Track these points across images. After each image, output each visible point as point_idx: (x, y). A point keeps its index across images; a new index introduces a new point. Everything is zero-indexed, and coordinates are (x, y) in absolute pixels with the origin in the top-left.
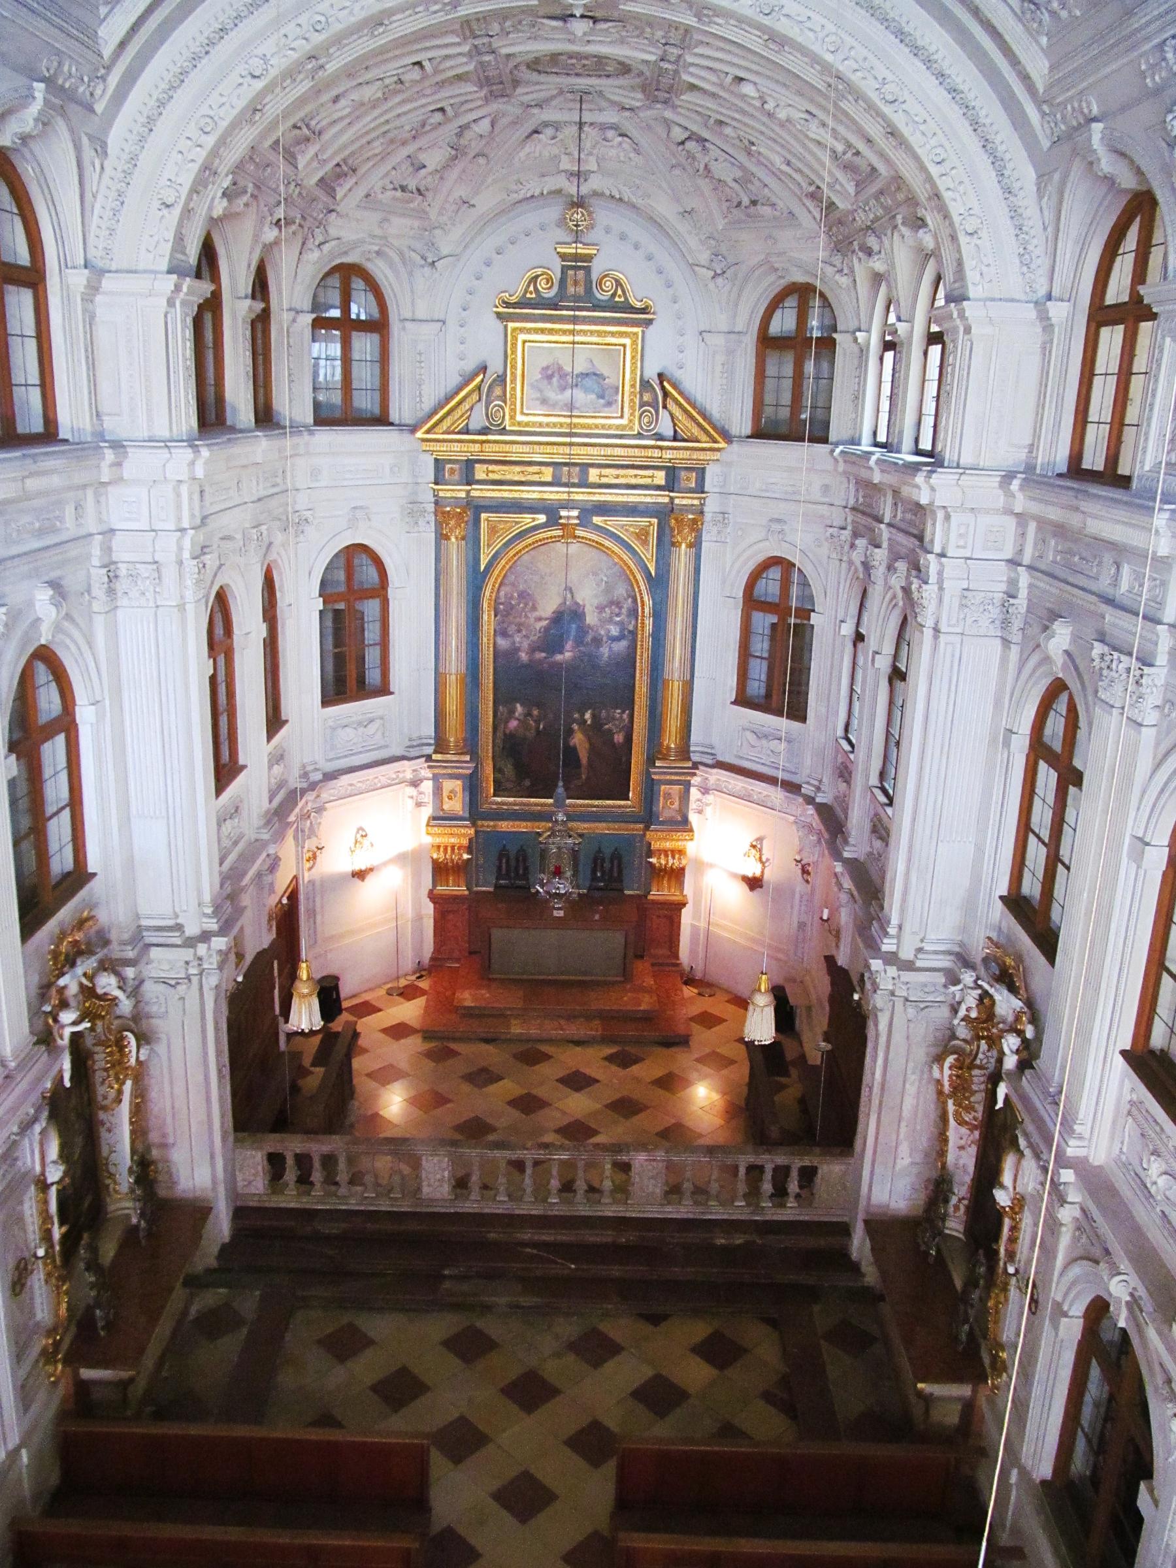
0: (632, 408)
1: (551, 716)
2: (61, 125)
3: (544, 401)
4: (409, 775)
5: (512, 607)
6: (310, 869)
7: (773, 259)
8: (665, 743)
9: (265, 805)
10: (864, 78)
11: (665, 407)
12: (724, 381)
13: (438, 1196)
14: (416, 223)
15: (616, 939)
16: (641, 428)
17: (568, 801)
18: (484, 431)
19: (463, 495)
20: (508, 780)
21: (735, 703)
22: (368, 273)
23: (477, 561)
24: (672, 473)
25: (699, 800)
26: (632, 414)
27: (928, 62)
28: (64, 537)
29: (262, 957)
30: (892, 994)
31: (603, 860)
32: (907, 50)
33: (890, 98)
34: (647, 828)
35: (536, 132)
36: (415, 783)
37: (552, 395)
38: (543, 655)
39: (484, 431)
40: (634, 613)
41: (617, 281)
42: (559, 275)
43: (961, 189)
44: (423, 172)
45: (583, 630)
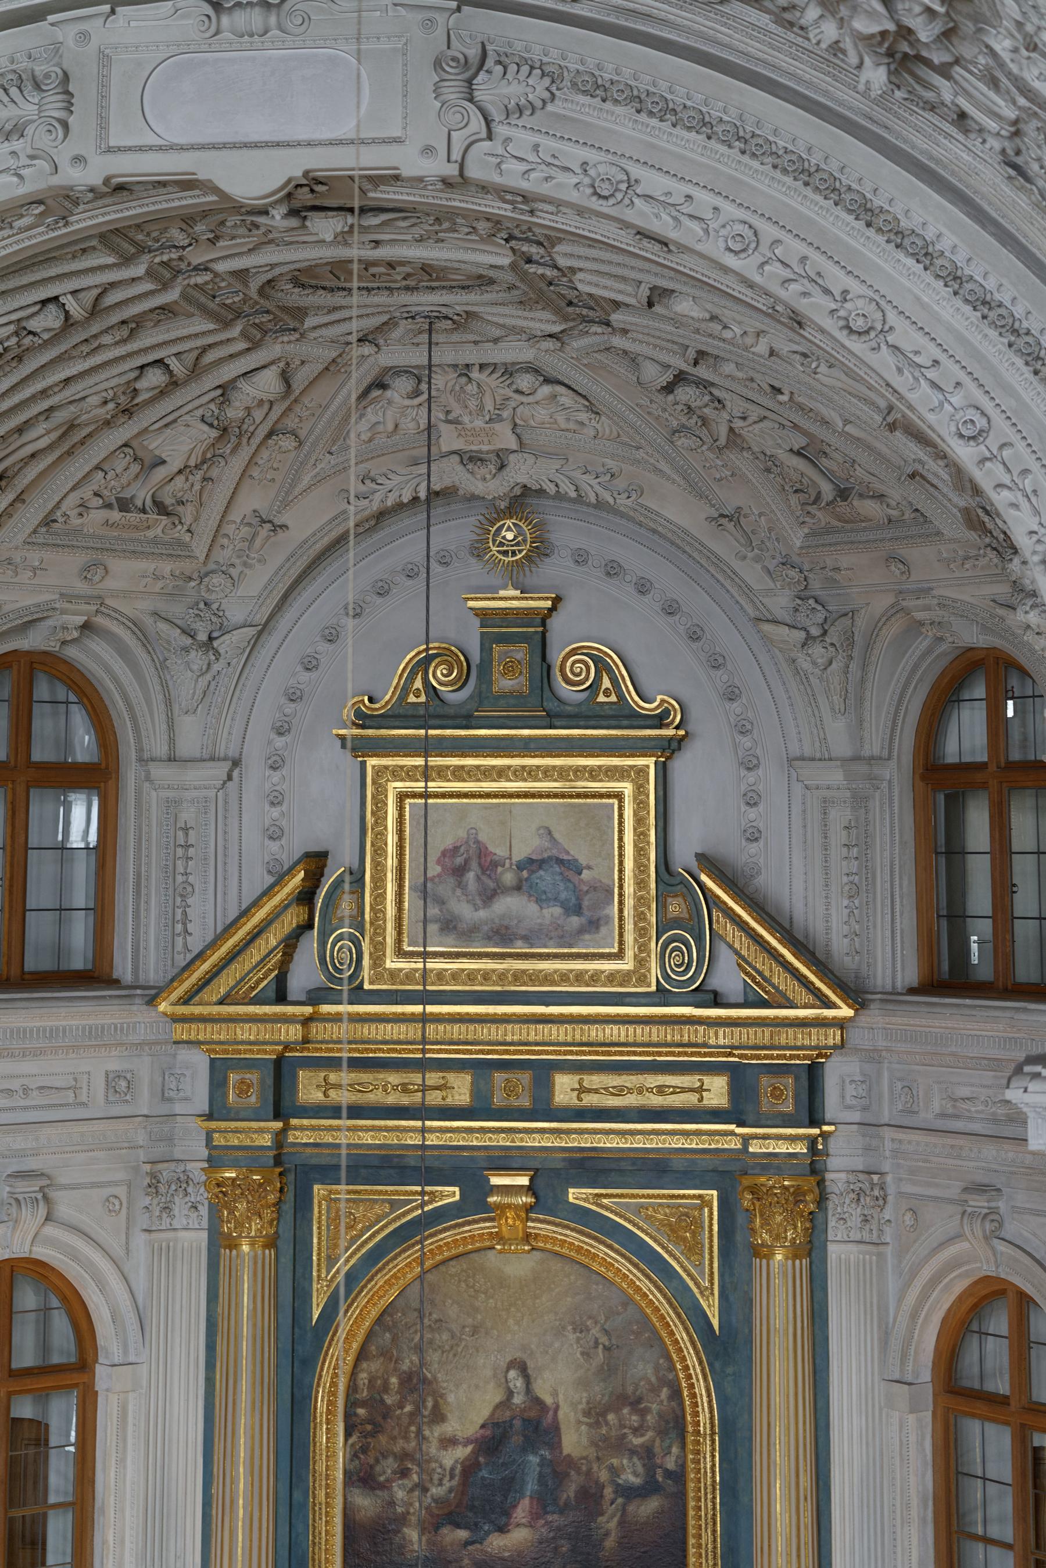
3: (449, 925)
10: (805, 294)
16: (666, 978)
18: (316, 997)
27: (926, 256)
32: (881, 239)
33: (859, 324)
37: (466, 912)
41: (596, 660)
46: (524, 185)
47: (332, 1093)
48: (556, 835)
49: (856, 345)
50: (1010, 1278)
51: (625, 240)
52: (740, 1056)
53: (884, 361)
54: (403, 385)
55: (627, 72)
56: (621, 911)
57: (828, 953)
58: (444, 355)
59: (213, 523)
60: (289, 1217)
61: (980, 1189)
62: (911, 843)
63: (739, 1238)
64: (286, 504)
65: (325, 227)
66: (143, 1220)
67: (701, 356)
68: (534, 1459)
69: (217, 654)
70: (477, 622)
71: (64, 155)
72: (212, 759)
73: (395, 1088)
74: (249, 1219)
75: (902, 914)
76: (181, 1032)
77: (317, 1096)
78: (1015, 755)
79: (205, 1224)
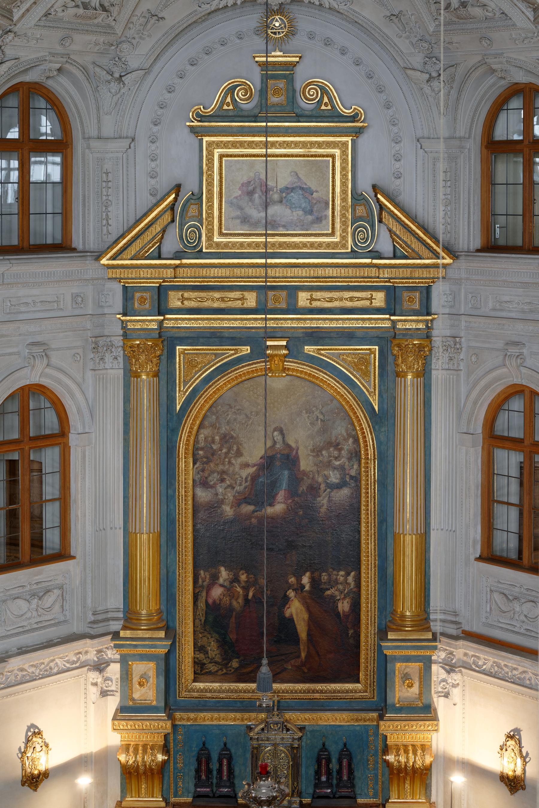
0: (344, 223)
3: (245, 220)
4: (92, 656)
8: (400, 610)
11: (380, 221)
16: (356, 245)
20: (212, 661)
21: (481, 559)
22: (49, 90)
23: (171, 399)
25: (444, 680)
26: (345, 231)
31: (329, 761)
39: (178, 255)
41: (321, 88)
42: (259, 85)
47: (186, 302)
48: (300, 176)
50: (528, 385)
52: (393, 283)
56: (333, 213)
59: (127, 16)
61: (516, 344)
62: (479, 180)
64: (166, 6)
66: (91, 365)
69: (124, 84)
70: (258, 69)
72: (120, 138)
73: (218, 299)
74: (147, 363)
75: (474, 214)
76: (111, 273)
77: (178, 304)
79: (121, 366)
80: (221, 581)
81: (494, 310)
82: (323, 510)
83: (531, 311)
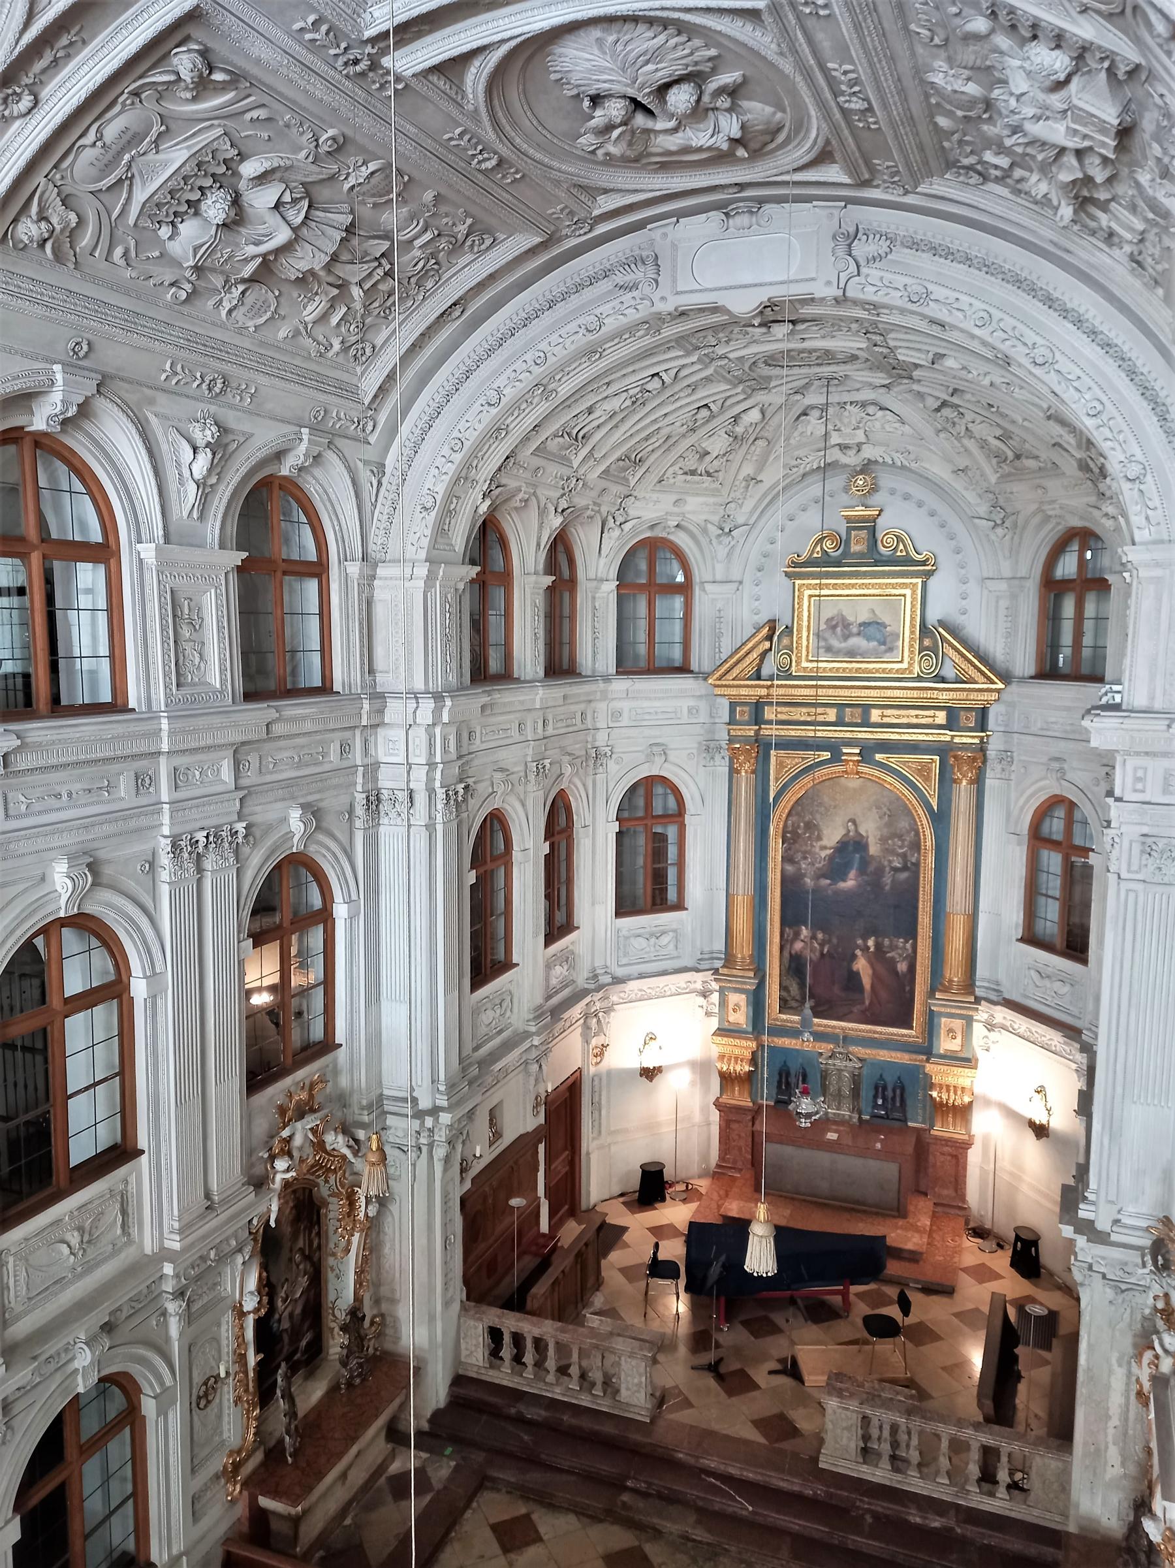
0: (911, 652)
1: (835, 941)
2: (331, 456)
3: (829, 649)
4: (699, 986)
5: (799, 836)
6: (597, 1064)
7: (1045, 507)
9: (539, 1000)
10: (1014, 346)
12: (1009, 625)
13: (634, 1401)
14: (711, 500)
15: (890, 1170)
17: (816, 1020)
19: (752, 733)
20: (794, 999)
21: (1022, 940)
24: (952, 713)
25: (986, 1037)
27: (1078, 322)
28: (327, 767)
29: (526, 1143)
30: (1090, 1268)
31: (885, 1088)
33: (1040, 360)
34: (928, 1061)
35: (805, 414)
36: (705, 994)
37: (835, 643)
38: (828, 881)
39: (771, 678)
40: (916, 846)
43: (1121, 437)
44: (708, 459)
45: (865, 862)
46: (875, 298)
49: (1037, 371)
51: (923, 326)
53: (1052, 379)
54: (816, 413)
55: (929, 234)
57: (994, 661)
58: (834, 398)
60: (761, 763)
63: (947, 776)
65: (780, 330)
66: (703, 762)
67: (955, 391)
68: (857, 856)
71: (656, 297)
78: (1089, 576)
80: (802, 937)
81: (1042, 729)
82: (887, 888)
83: (1074, 732)
